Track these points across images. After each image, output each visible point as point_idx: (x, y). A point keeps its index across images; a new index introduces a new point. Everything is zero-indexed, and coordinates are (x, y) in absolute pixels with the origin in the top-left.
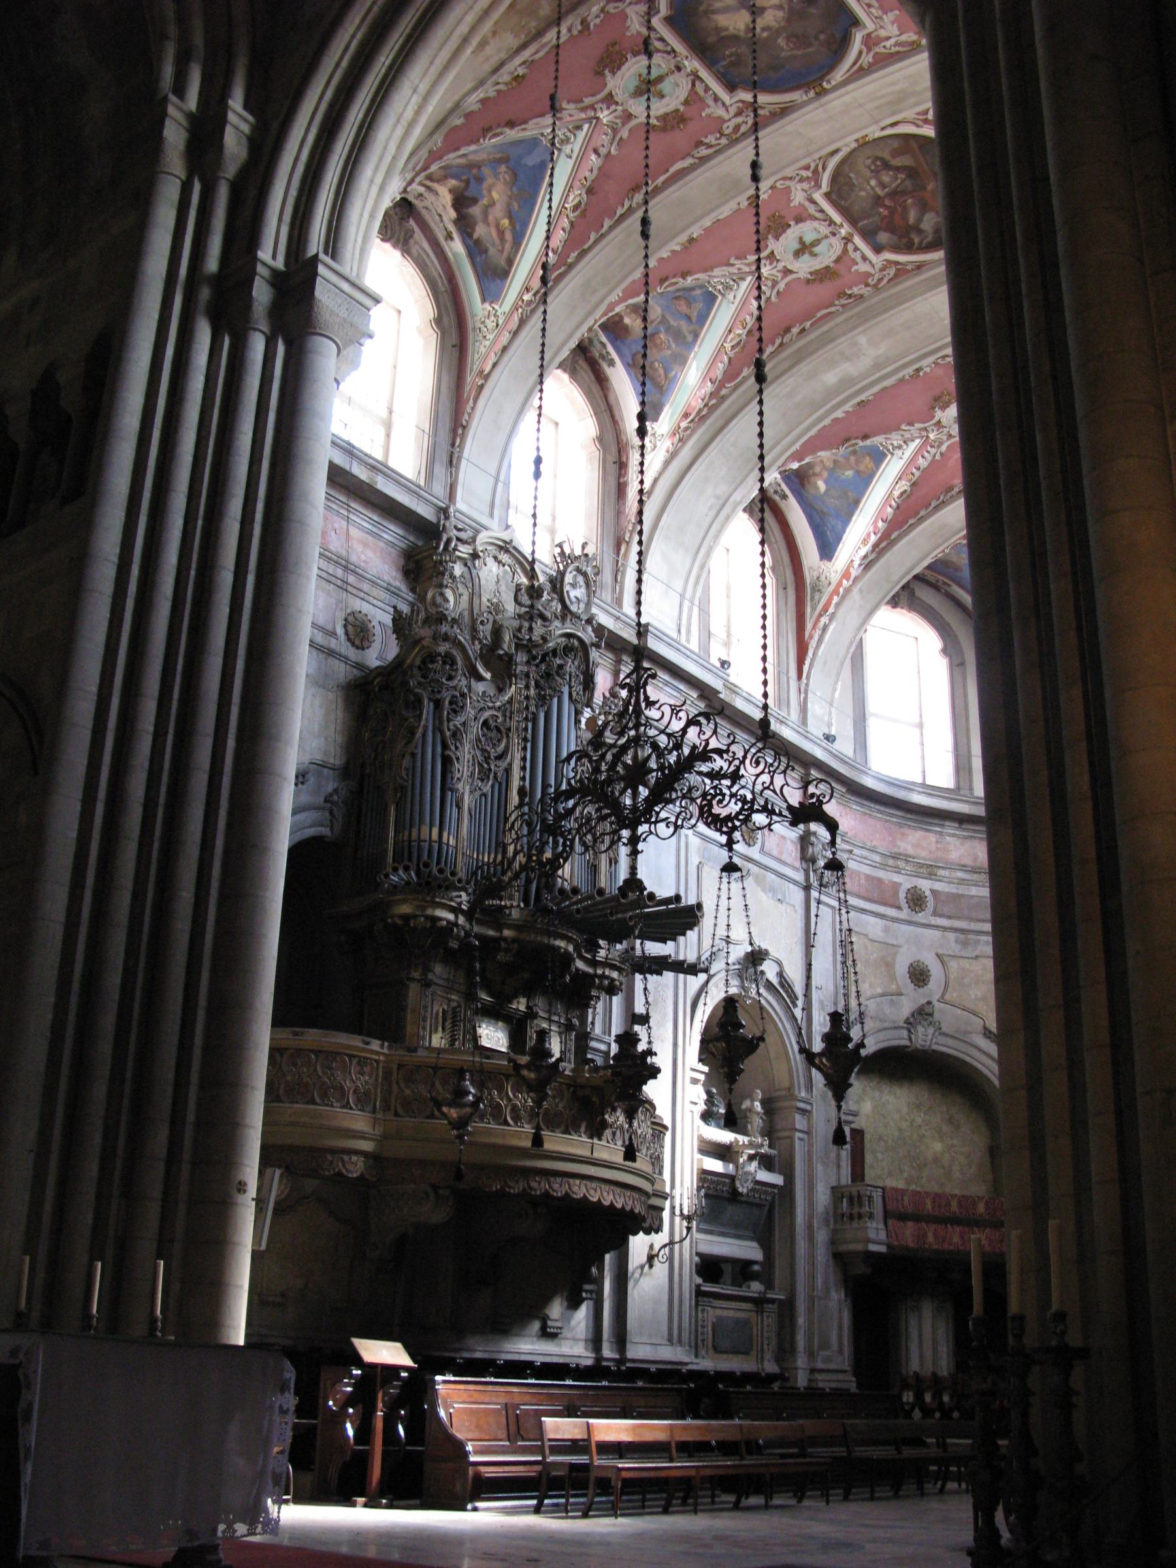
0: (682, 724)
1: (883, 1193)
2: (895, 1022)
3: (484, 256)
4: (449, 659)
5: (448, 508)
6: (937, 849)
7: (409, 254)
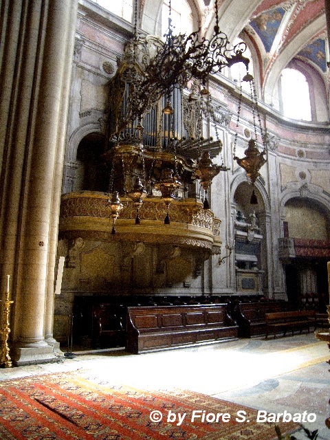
4: (133, 70)
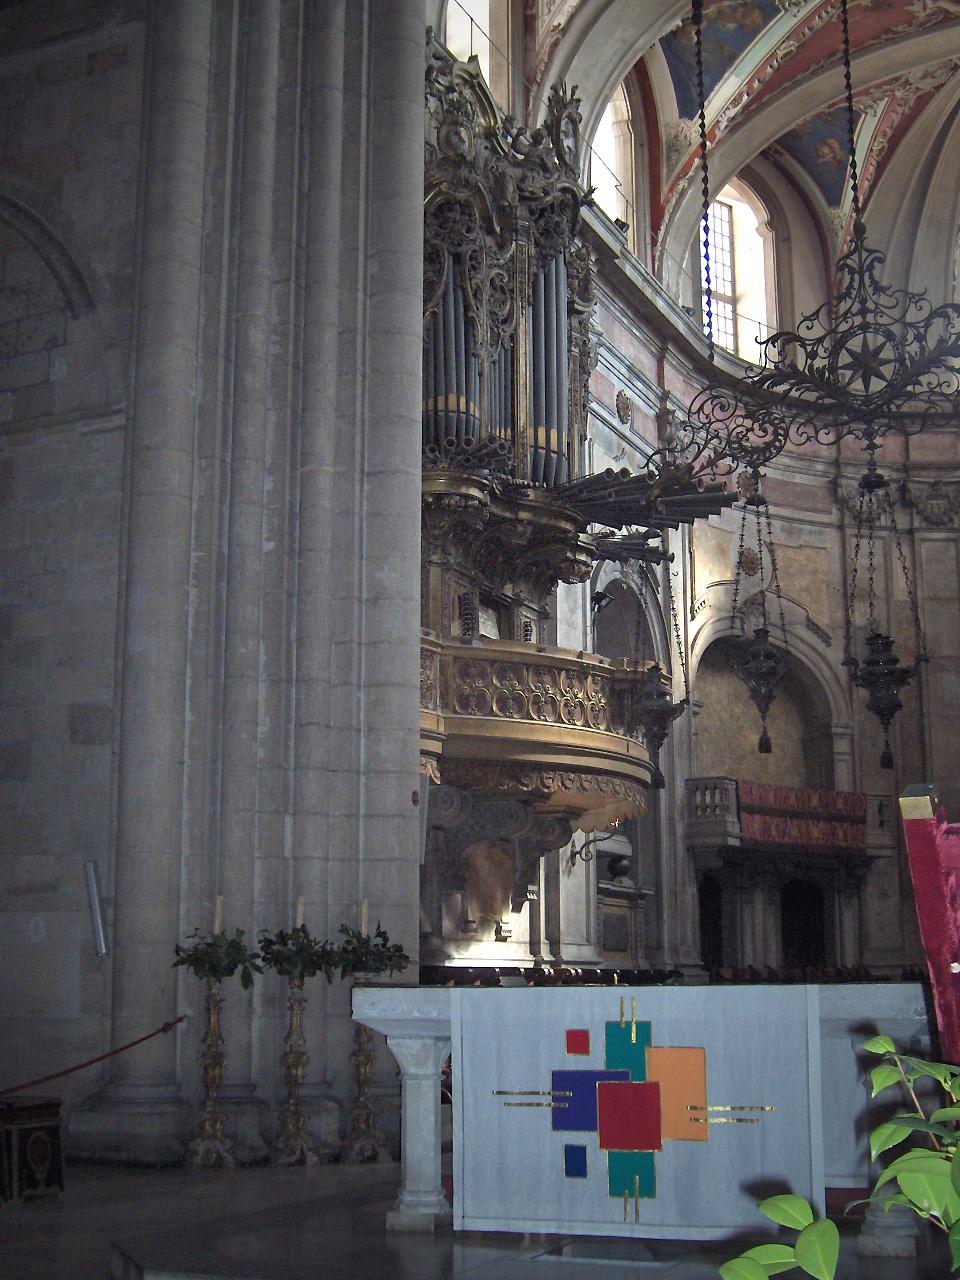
0: (925, 313)
1: (737, 787)
4: (466, 208)
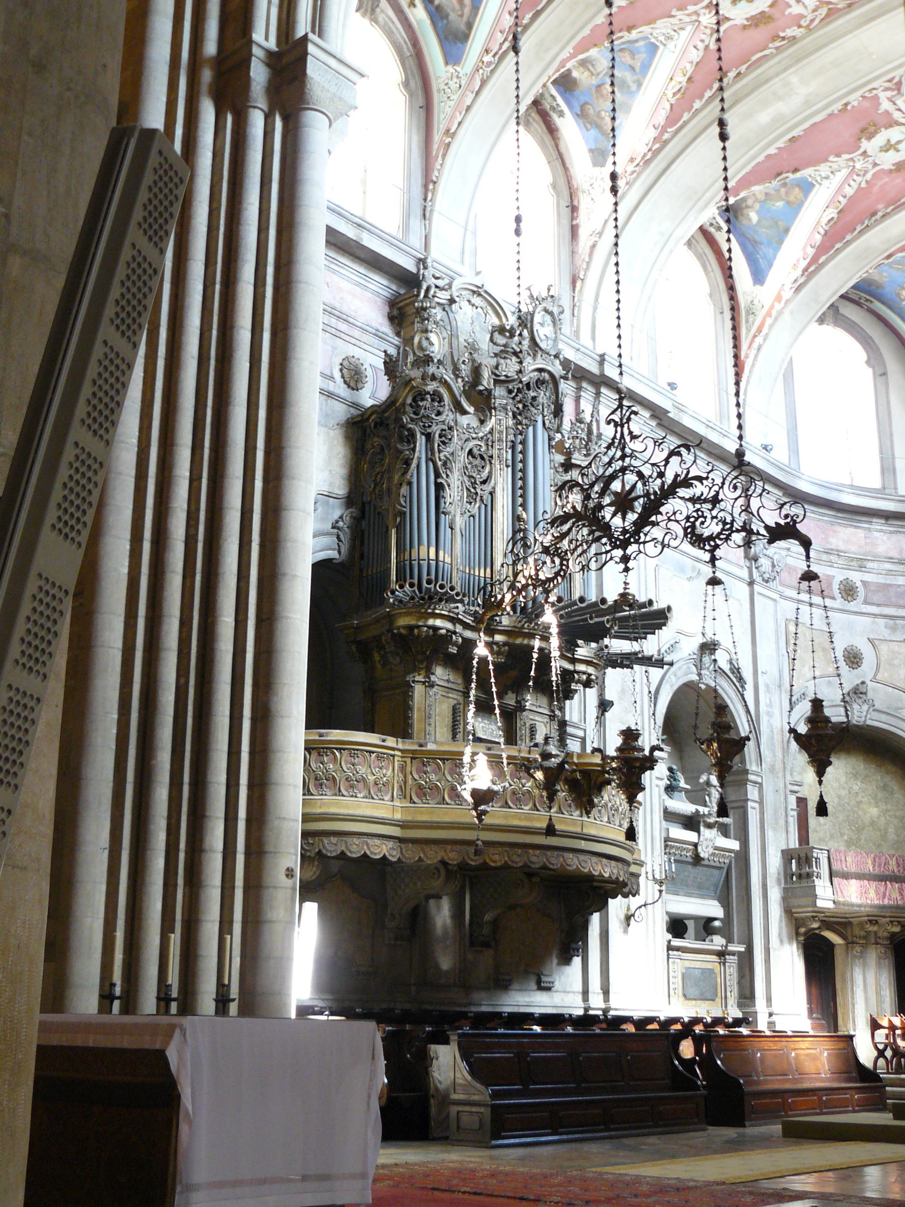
2: (832, 701)
3: (445, 21)
4: (437, 397)
5: (426, 258)
6: (866, 544)
7: (376, 22)
